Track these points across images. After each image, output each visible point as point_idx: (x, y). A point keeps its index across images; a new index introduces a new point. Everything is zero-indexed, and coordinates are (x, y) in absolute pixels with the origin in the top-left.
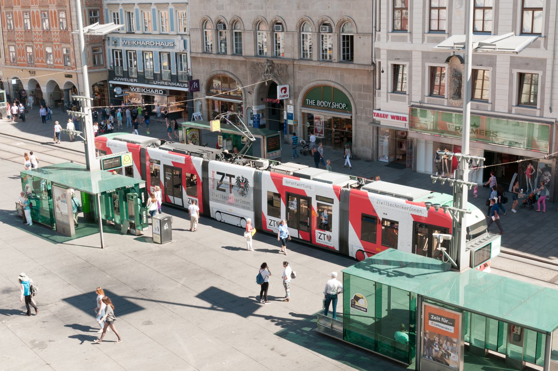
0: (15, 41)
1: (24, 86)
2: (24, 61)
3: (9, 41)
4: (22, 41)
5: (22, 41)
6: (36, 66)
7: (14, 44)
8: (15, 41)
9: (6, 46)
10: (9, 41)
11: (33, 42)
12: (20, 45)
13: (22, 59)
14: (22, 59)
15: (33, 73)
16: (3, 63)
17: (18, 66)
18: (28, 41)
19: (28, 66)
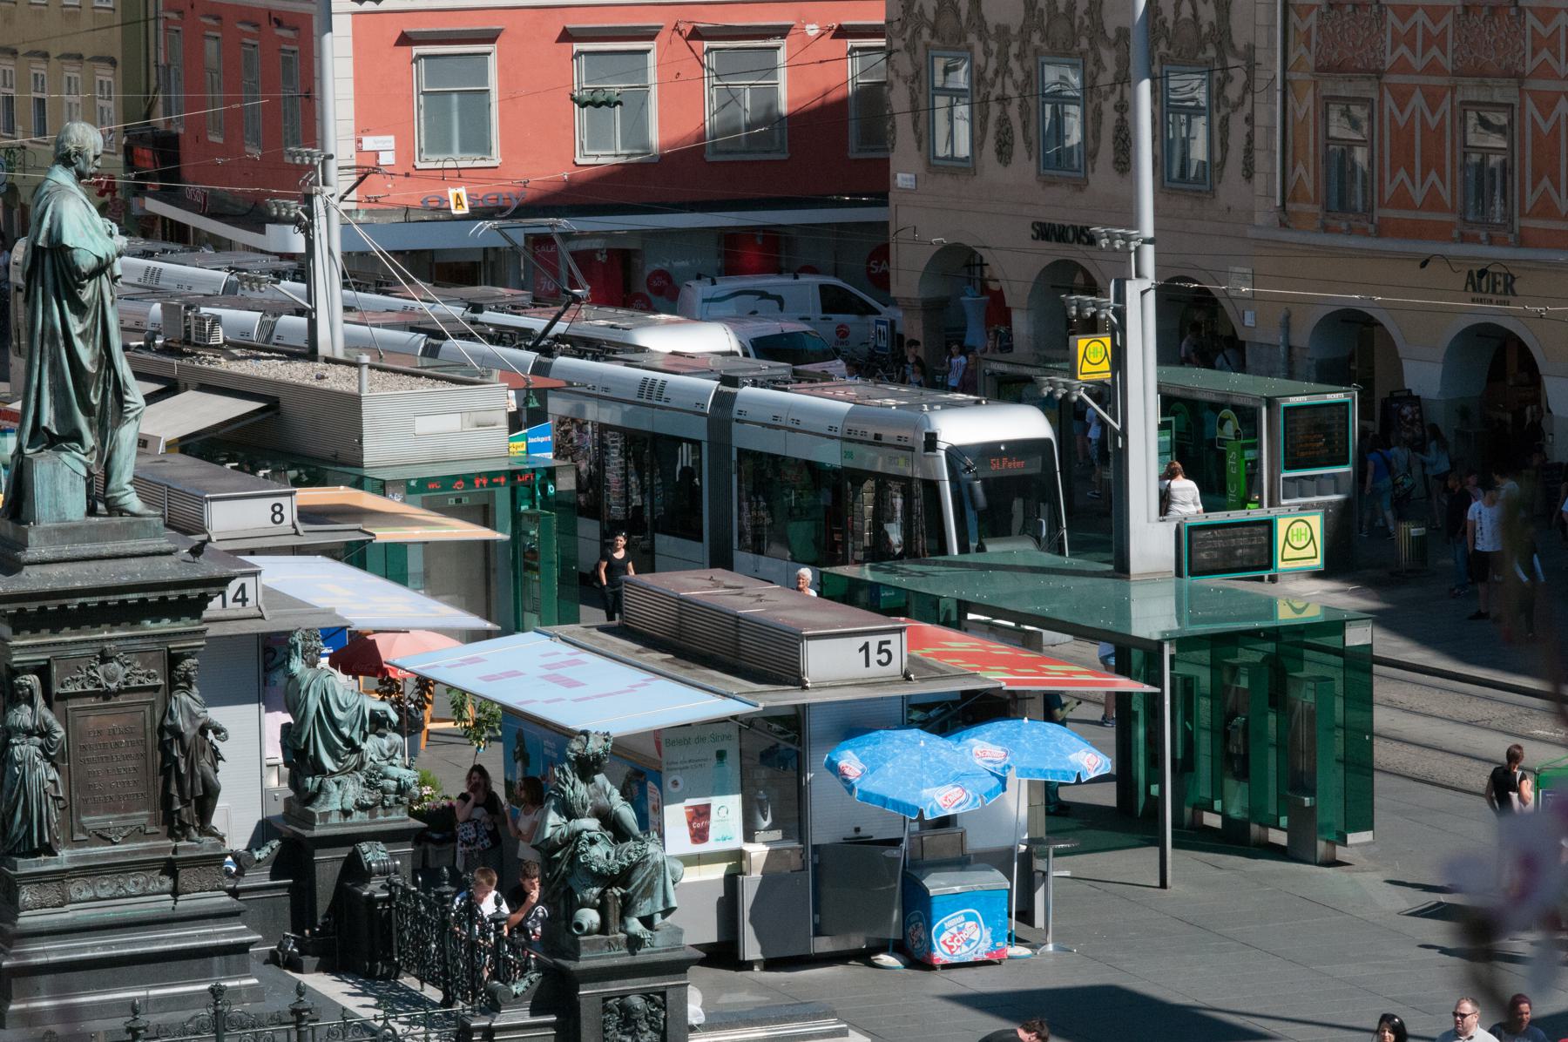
0: (1379, 74)
1: (1408, 367)
2: (1433, 201)
3: (1325, 68)
4: (1433, 68)
5: (1433, 68)
6: (1522, 242)
7: (1367, 88)
8: (1379, 74)
9: (1305, 105)
10: (1325, 68)
11: (1520, 77)
12: (1417, 100)
13: (1418, 194)
14: (1418, 194)
15: (1480, 280)
16: (1264, 214)
17: (1380, 232)
18: (1480, 73)
19: (1464, 238)
